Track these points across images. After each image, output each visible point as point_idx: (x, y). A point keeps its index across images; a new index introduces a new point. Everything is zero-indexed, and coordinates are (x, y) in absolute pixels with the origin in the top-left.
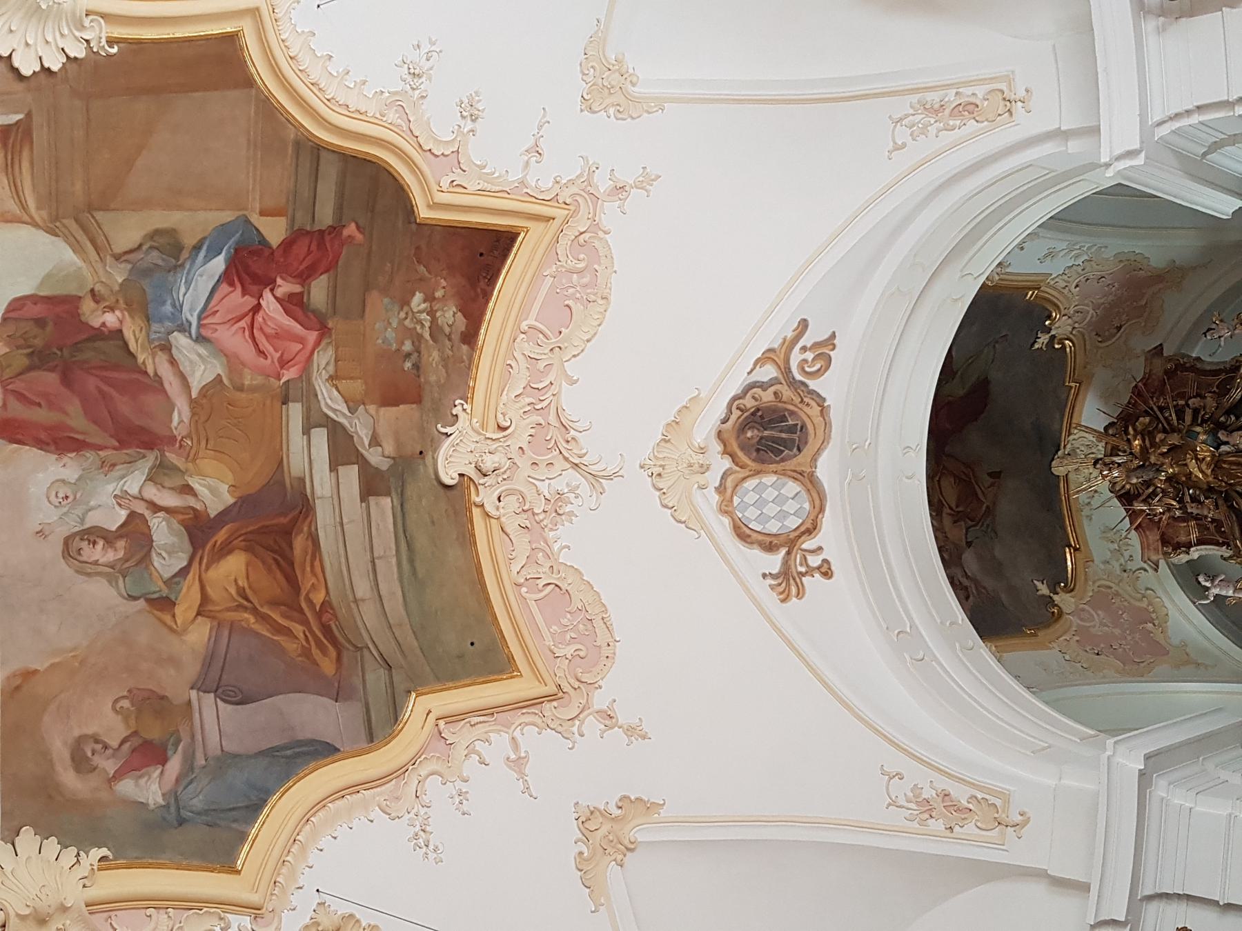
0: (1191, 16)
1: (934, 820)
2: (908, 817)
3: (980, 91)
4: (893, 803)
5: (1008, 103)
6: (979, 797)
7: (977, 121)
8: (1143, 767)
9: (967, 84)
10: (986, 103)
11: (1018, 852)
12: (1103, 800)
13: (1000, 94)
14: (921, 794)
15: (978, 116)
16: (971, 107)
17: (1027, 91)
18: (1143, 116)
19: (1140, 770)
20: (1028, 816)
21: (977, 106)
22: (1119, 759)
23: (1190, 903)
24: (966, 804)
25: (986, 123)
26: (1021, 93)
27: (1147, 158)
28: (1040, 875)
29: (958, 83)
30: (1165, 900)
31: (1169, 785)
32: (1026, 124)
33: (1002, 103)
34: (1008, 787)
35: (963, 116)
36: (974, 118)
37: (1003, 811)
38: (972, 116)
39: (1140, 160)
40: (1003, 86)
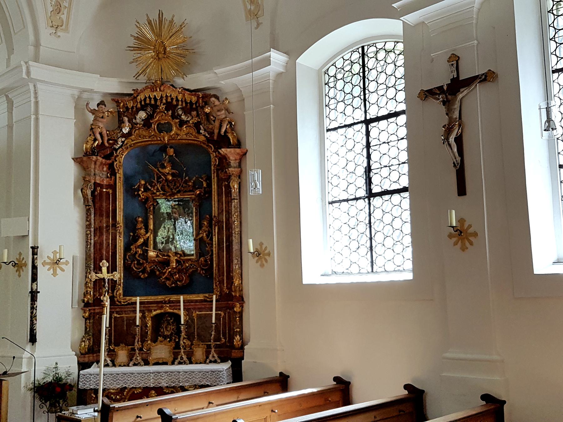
0: (75, 107)
3: (64, 17)
5: (56, 27)
7: (52, 11)
9: (69, 13)
10: (58, 18)
13: (60, 24)
15: (54, 13)
16: (58, 11)
17: (59, 36)
18: (39, 81)
21: (58, 14)
25: (50, 15)
26: (59, 33)
27: (24, 78)
29: (70, 8)
32: (45, 32)
33: (57, 24)
35: (56, 6)
36: (53, 11)
38: (55, 10)
39: (24, 76)
40: (64, 27)
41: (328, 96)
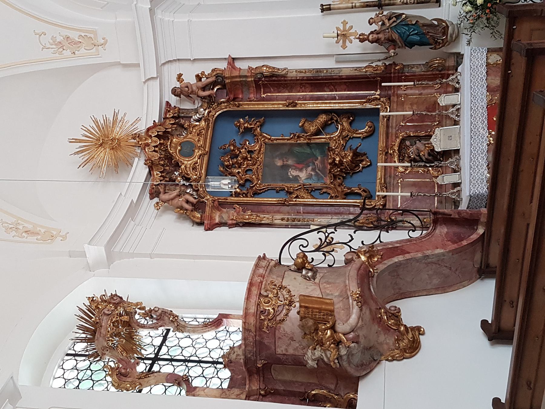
1: (65, 51)
2: (52, 52)
4: (44, 47)
6: (83, 35)
8: (150, 7)
11: (106, 56)
12: (137, 25)
14: (56, 40)
19: (149, 8)
20: (106, 39)
22: (139, 5)
23: (180, 62)
24: (77, 39)
28: (118, 64)
30: (170, 63)
31: (162, 11)
34: (94, 28)
37: (95, 39)
41: (151, 388)
